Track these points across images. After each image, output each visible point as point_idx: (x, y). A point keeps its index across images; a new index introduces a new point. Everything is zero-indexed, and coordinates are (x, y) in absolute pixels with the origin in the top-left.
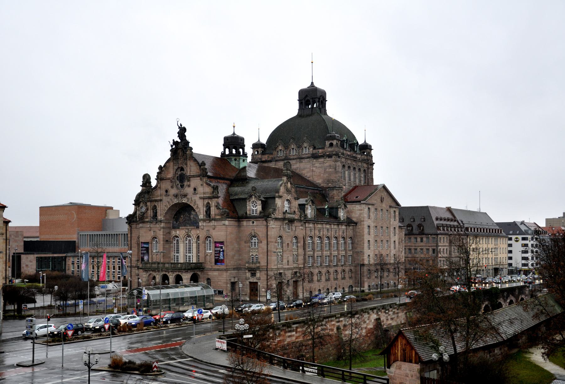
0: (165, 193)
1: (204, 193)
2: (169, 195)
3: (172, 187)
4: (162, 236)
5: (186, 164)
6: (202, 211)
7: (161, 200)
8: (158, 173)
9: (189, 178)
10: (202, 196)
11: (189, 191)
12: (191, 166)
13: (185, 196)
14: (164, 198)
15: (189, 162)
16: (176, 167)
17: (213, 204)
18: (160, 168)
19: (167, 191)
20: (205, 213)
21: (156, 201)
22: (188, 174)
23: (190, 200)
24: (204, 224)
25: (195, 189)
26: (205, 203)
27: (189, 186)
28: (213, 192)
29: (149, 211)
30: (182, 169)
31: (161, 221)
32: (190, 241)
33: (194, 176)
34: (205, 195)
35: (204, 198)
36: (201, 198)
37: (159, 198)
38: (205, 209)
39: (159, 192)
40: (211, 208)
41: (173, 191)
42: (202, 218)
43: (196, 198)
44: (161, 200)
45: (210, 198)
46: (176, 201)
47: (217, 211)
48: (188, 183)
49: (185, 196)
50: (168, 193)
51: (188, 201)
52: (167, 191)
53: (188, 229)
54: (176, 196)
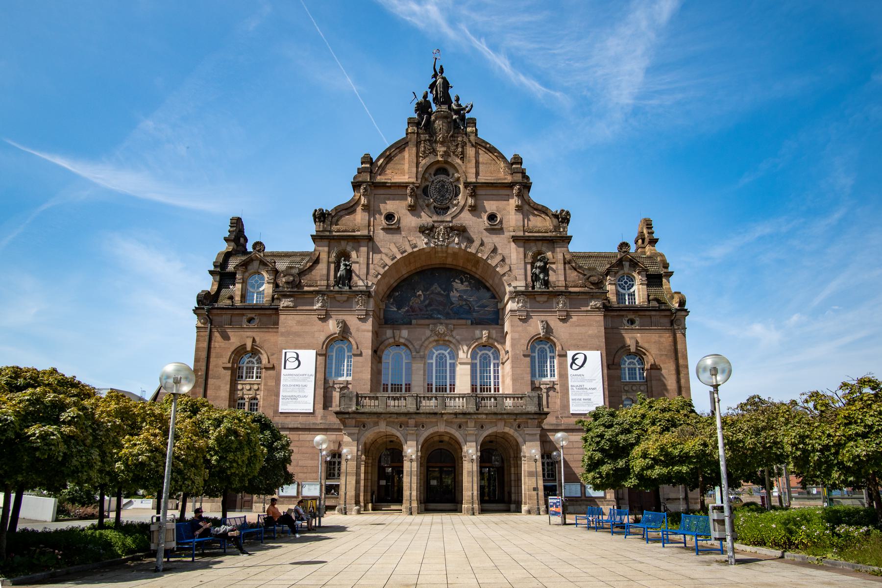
4: (370, 334)
6: (518, 272)
8: (360, 171)
10: (521, 234)
12: (477, 163)
15: (471, 152)
16: (424, 162)
17: (560, 256)
18: (367, 159)
20: (529, 279)
22: (472, 179)
23: (477, 243)
28: (557, 228)
30: (442, 169)
31: (367, 294)
32: (441, 357)
34: (527, 234)
36: (515, 239)
38: (529, 267)
39: (360, 217)
41: (409, 221)
42: (523, 289)
53: (447, 325)
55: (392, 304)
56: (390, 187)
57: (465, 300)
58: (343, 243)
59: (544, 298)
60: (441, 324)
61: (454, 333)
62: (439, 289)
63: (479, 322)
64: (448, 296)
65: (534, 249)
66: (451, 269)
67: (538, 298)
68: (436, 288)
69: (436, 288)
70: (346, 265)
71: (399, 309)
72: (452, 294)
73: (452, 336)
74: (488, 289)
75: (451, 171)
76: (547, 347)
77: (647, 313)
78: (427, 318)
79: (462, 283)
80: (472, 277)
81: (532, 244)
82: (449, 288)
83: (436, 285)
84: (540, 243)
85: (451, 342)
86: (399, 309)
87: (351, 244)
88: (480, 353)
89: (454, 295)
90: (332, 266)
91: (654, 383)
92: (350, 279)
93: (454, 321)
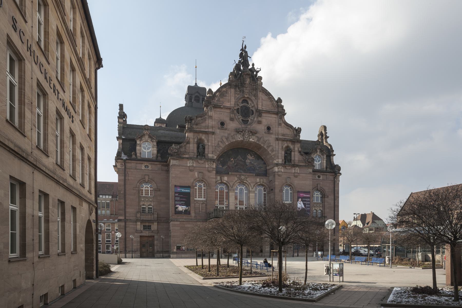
0: (220, 126)
1: (283, 135)
2: (226, 129)
3: (232, 119)
5: (256, 96)
7: (213, 133)
9: (260, 113)
11: (261, 128)
13: (253, 133)
14: (218, 131)
17: (296, 149)
19: (222, 124)
20: (283, 158)
21: (206, 133)
24: (283, 170)
25: (269, 128)
26: (284, 146)
27: (260, 122)
29: (191, 145)
33: (268, 112)
35: (283, 140)
37: (210, 130)
40: (293, 153)
41: (232, 125)
43: (271, 139)
44: (213, 133)
45: (291, 141)
46: (239, 138)
47: (301, 157)
48: (260, 119)
49: (253, 133)
50: (225, 126)
51: (258, 140)
52: (222, 124)
54: (238, 131)
55: (220, 164)
56: (222, 108)
57: (253, 164)
58: (200, 134)
59: (290, 168)
60: (243, 175)
61: (248, 179)
62: (241, 158)
63: (258, 175)
64: (245, 162)
65: (286, 145)
66: (247, 149)
67: (287, 168)
68: (239, 157)
69: (239, 157)
70: (202, 146)
71: (223, 166)
72: (247, 161)
73: (247, 181)
74: (263, 160)
75: (250, 102)
76: (289, 188)
77: (325, 174)
78: (236, 172)
79: (251, 156)
80: (256, 154)
81: (285, 142)
82: (245, 158)
83: (239, 156)
84: (288, 142)
85: (246, 183)
86: (223, 166)
87: (204, 135)
88: (258, 189)
89: (248, 161)
90: (196, 145)
91: (326, 203)
92: (204, 152)
93: (248, 174)
